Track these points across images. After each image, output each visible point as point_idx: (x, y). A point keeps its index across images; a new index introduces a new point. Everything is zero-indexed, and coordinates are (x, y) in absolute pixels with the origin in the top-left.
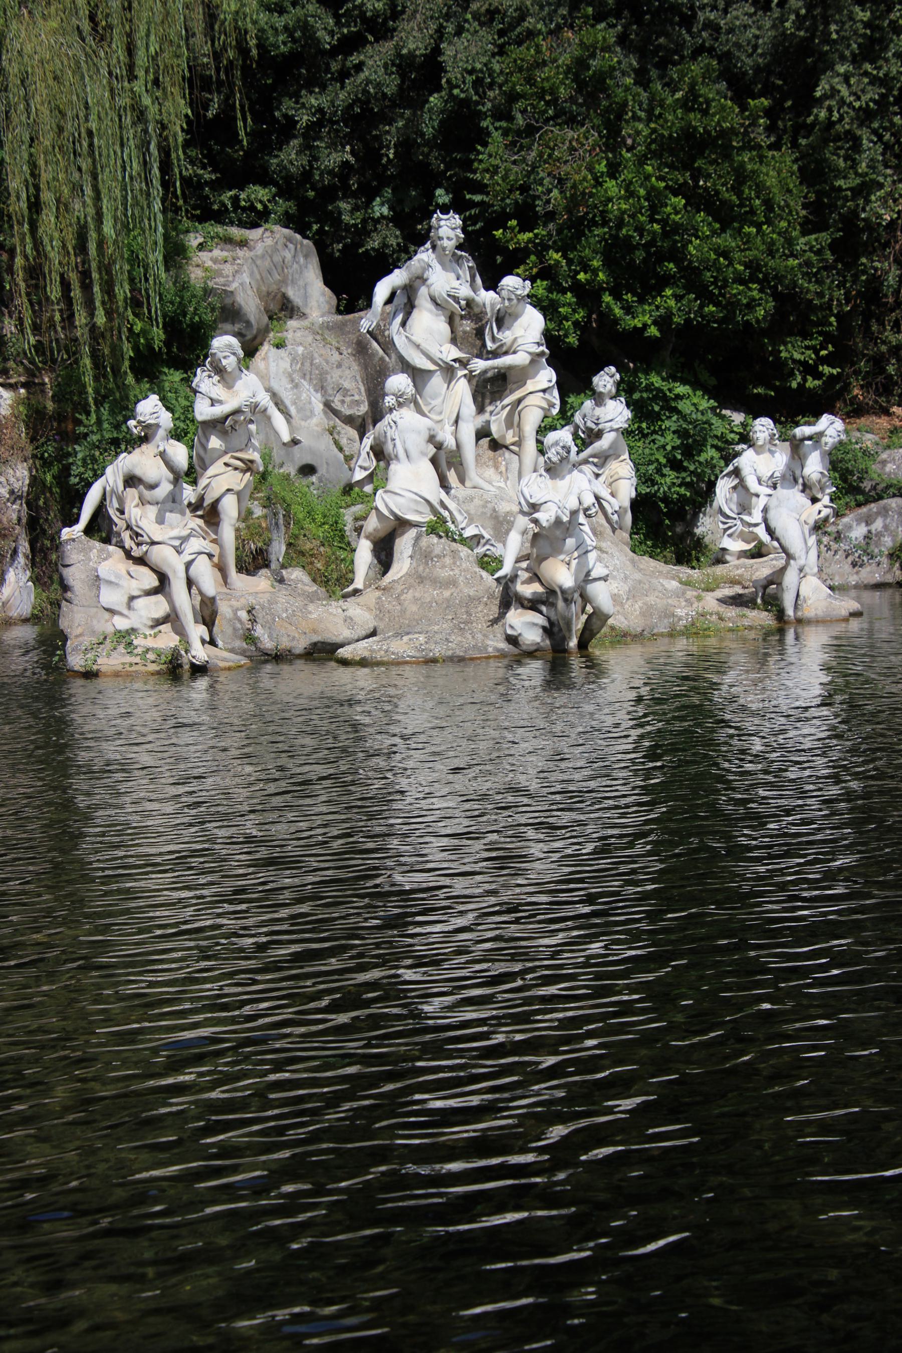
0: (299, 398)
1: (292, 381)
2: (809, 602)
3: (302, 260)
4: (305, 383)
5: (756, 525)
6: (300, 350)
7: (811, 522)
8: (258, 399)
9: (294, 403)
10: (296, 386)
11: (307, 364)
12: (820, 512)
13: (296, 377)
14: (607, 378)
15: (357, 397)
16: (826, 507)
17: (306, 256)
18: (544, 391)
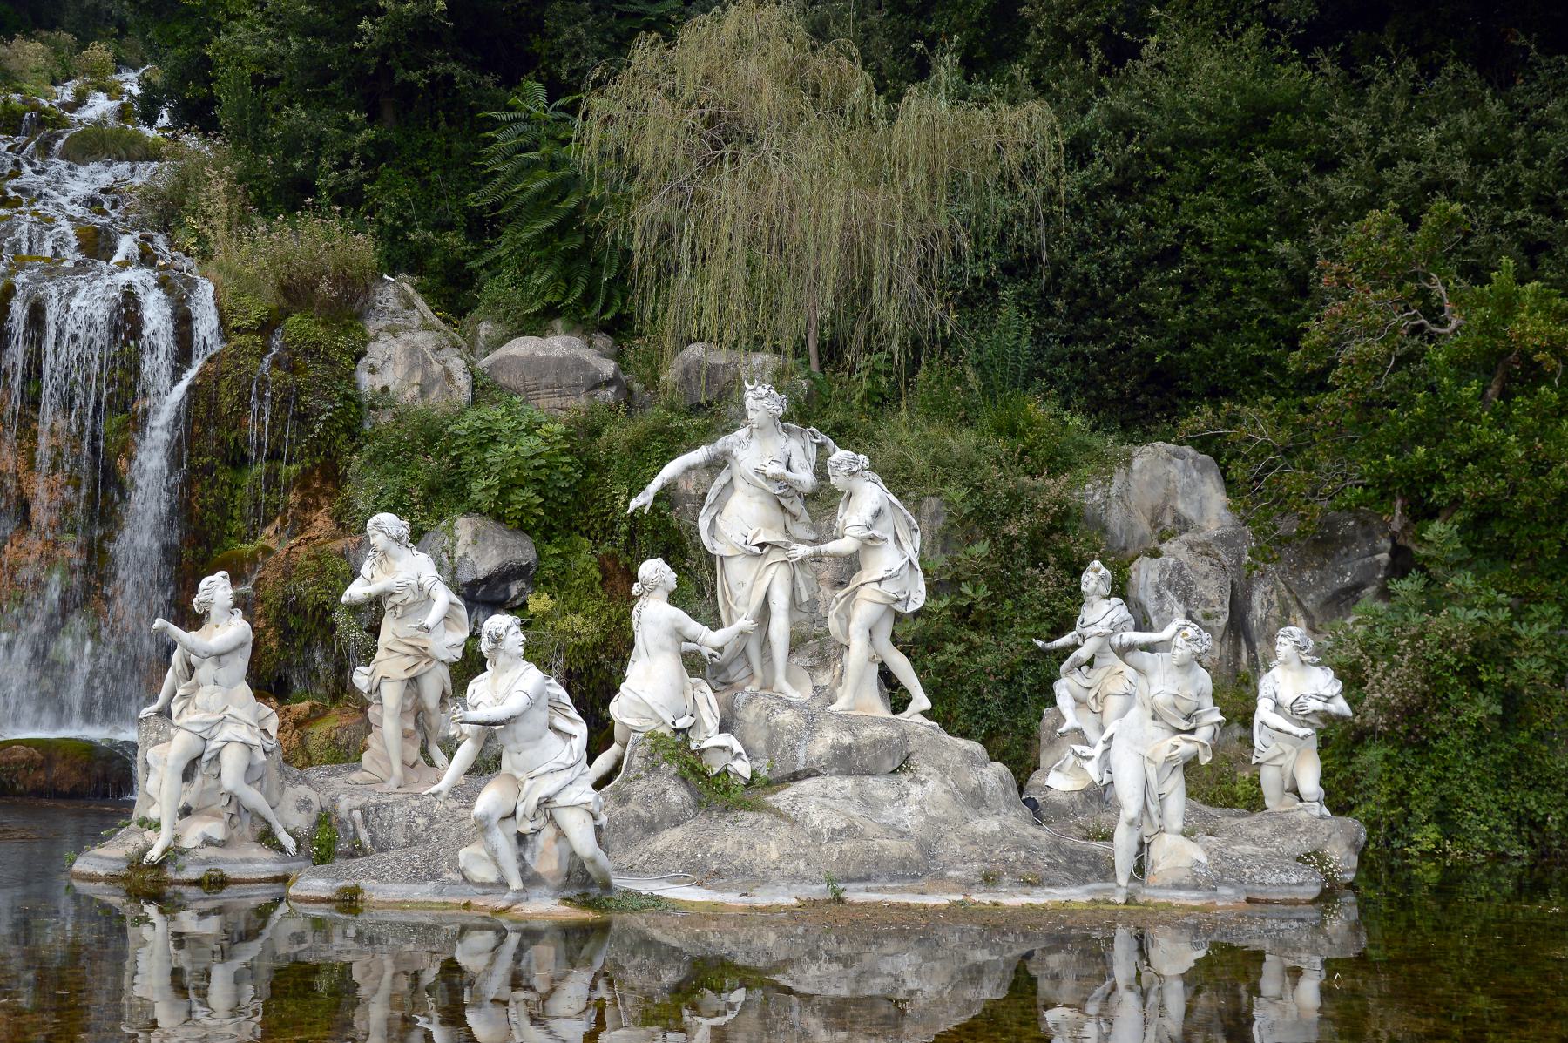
0: (1162, 609)
1: (1158, 591)
2: (1158, 869)
3: (1195, 474)
4: (1169, 595)
5: (1089, 758)
6: (1171, 561)
7: (1160, 758)
8: (422, 581)
9: (1156, 613)
10: (1160, 596)
11: (1175, 578)
12: (1177, 747)
13: (1163, 589)
14: (1091, 574)
15: (1218, 608)
16: (1189, 741)
17: (1201, 471)
18: (879, 581)
